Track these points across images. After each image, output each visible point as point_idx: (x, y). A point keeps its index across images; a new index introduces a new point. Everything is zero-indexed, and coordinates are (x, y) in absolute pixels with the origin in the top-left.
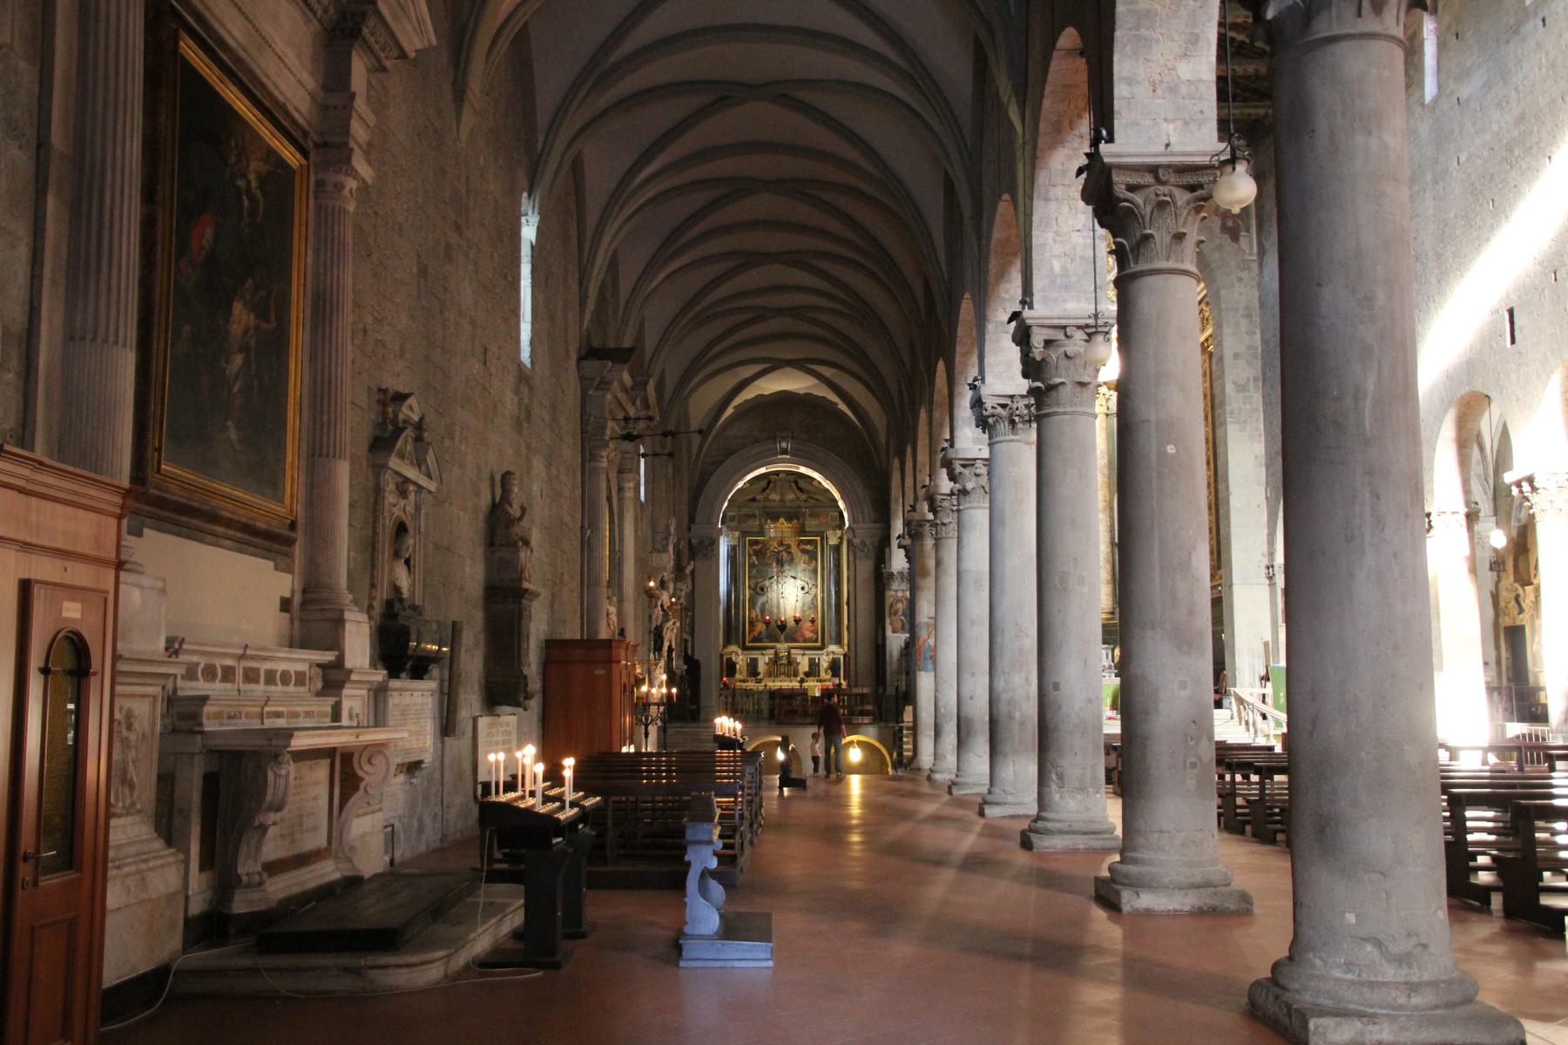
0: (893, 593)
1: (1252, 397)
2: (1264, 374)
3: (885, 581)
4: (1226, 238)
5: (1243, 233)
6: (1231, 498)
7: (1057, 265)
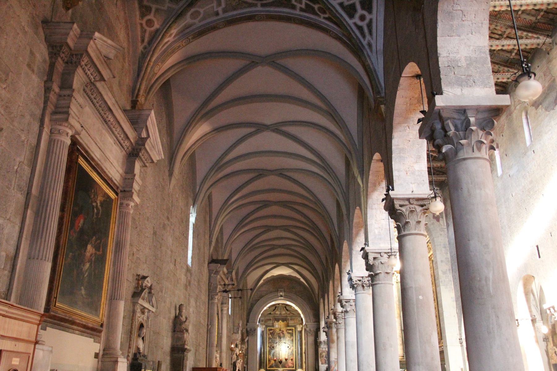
1: (449, 276)
2: (452, 268)
3: (318, 344)
4: (435, 221)
5: (441, 219)
6: (444, 313)
7: (376, 231)
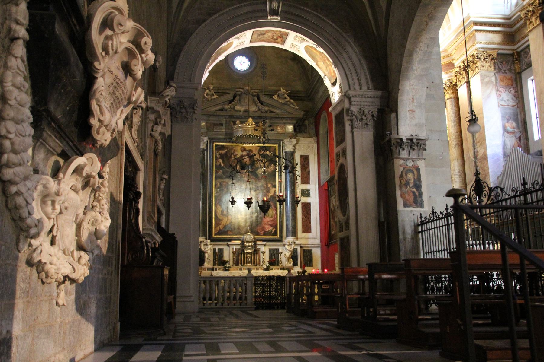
0: (401, 162)
3: (393, 148)
